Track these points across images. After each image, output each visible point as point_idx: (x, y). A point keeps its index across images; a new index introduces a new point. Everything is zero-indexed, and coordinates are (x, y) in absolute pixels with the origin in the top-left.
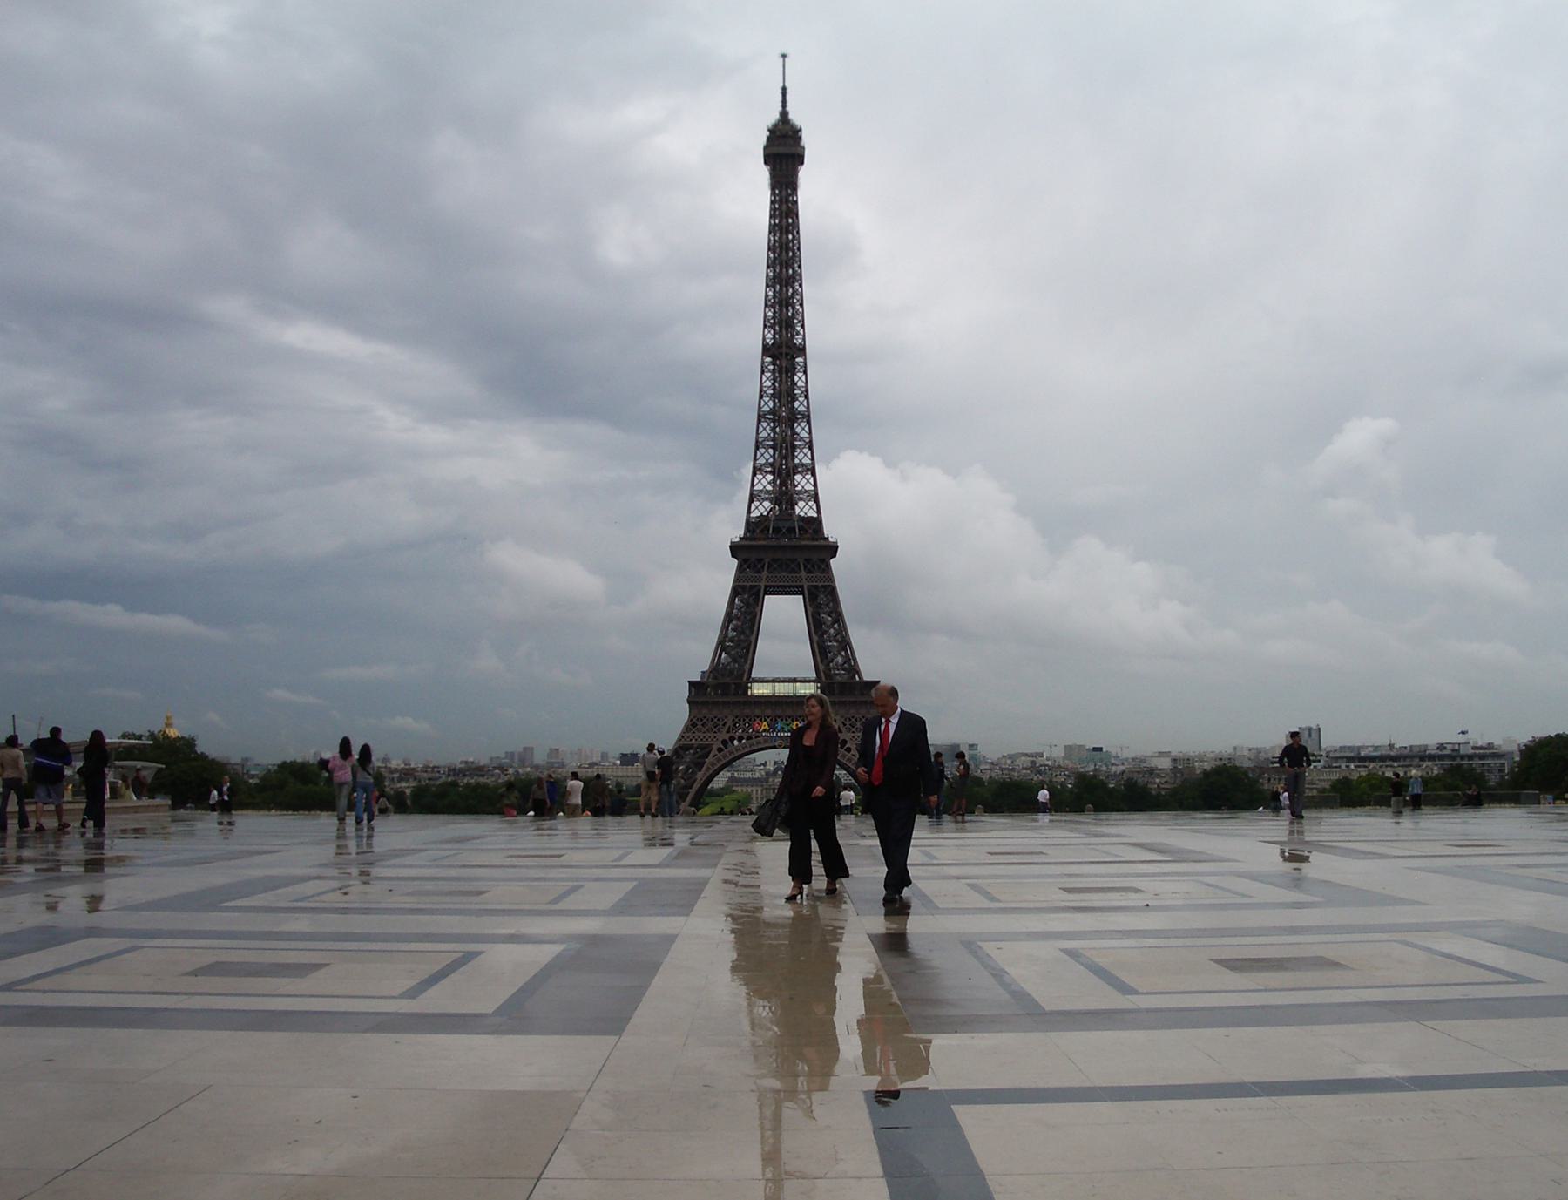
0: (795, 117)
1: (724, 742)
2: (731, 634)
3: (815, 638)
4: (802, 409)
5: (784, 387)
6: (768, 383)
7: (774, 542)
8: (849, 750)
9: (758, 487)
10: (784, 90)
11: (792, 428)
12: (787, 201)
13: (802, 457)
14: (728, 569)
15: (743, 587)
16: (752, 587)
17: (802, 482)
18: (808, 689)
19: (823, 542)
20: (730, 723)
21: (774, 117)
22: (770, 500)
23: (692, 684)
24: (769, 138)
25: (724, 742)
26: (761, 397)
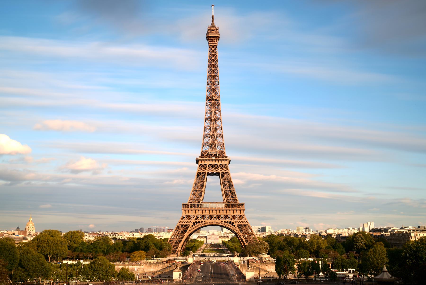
0: (216, 24)
1: (194, 224)
2: (196, 188)
3: (224, 189)
4: (219, 116)
5: (213, 109)
6: (208, 109)
7: (209, 159)
8: (234, 226)
9: (205, 141)
10: (213, 16)
11: (216, 122)
12: (214, 51)
13: (219, 131)
14: (195, 169)
15: (200, 173)
16: (203, 173)
17: (219, 139)
18: (222, 206)
19: (225, 159)
20: (196, 217)
21: (210, 25)
22: (209, 146)
23: (184, 205)
24: (208, 32)
25: (194, 224)
26: (206, 113)
